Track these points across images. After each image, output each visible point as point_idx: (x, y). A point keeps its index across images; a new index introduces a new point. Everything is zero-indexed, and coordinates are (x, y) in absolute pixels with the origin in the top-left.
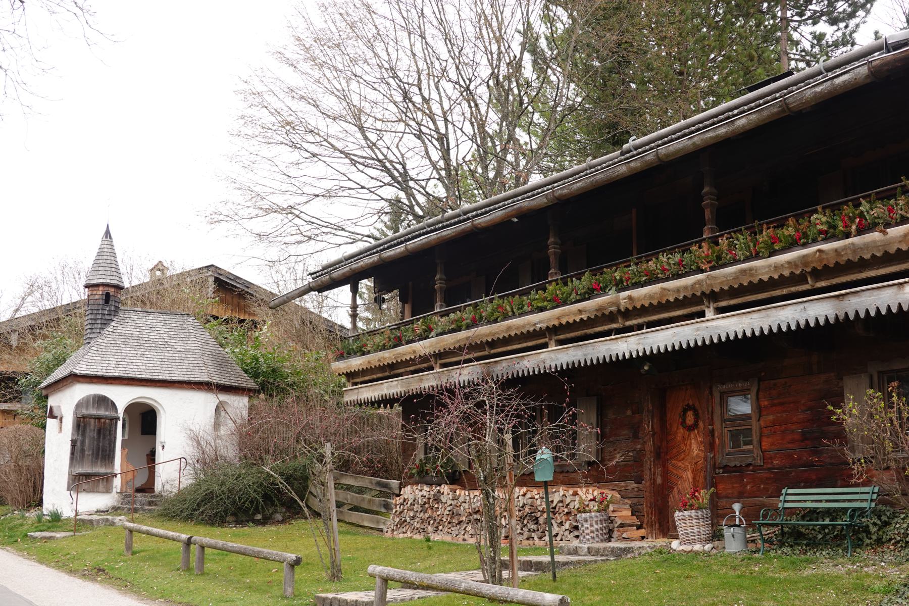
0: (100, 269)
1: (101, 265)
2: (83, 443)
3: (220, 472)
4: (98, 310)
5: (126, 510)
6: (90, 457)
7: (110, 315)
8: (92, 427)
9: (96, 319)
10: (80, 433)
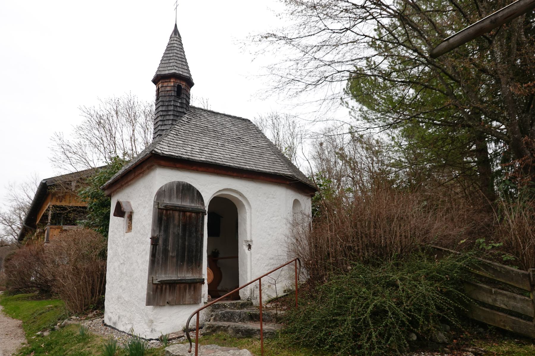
0: (170, 61)
1: (172, 58)
2: (166, 241)
3: (436, 285)
4: (170, 101)
5: (230, 331)
6: (175, 260)
7: (182, 107)
8: (176, 222)
9: (167, 111)
10: (163, 228)
